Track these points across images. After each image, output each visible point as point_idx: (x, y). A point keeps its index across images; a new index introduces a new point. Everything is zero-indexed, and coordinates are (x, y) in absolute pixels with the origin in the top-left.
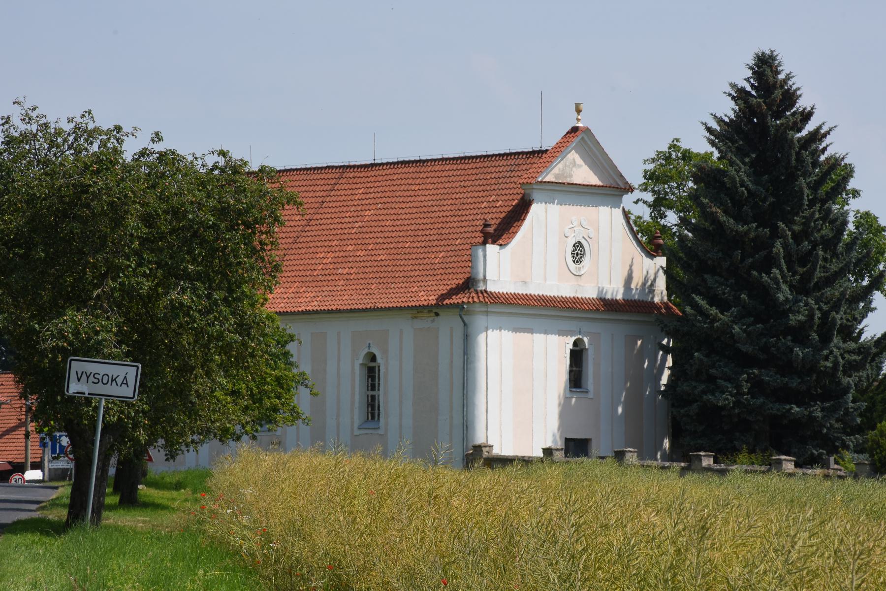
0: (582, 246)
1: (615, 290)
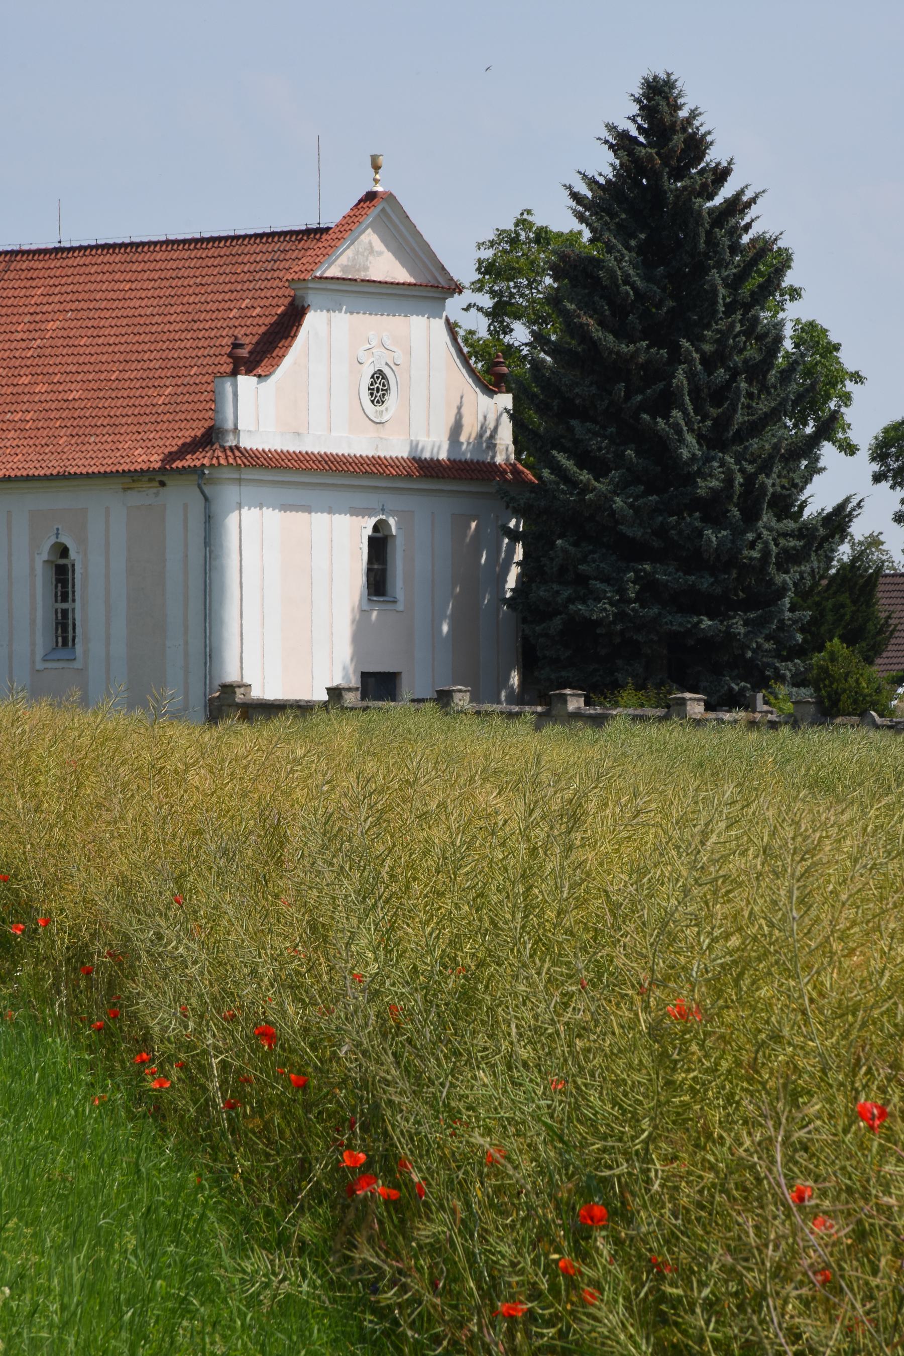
0: (384, 377)
1: (436, 446)
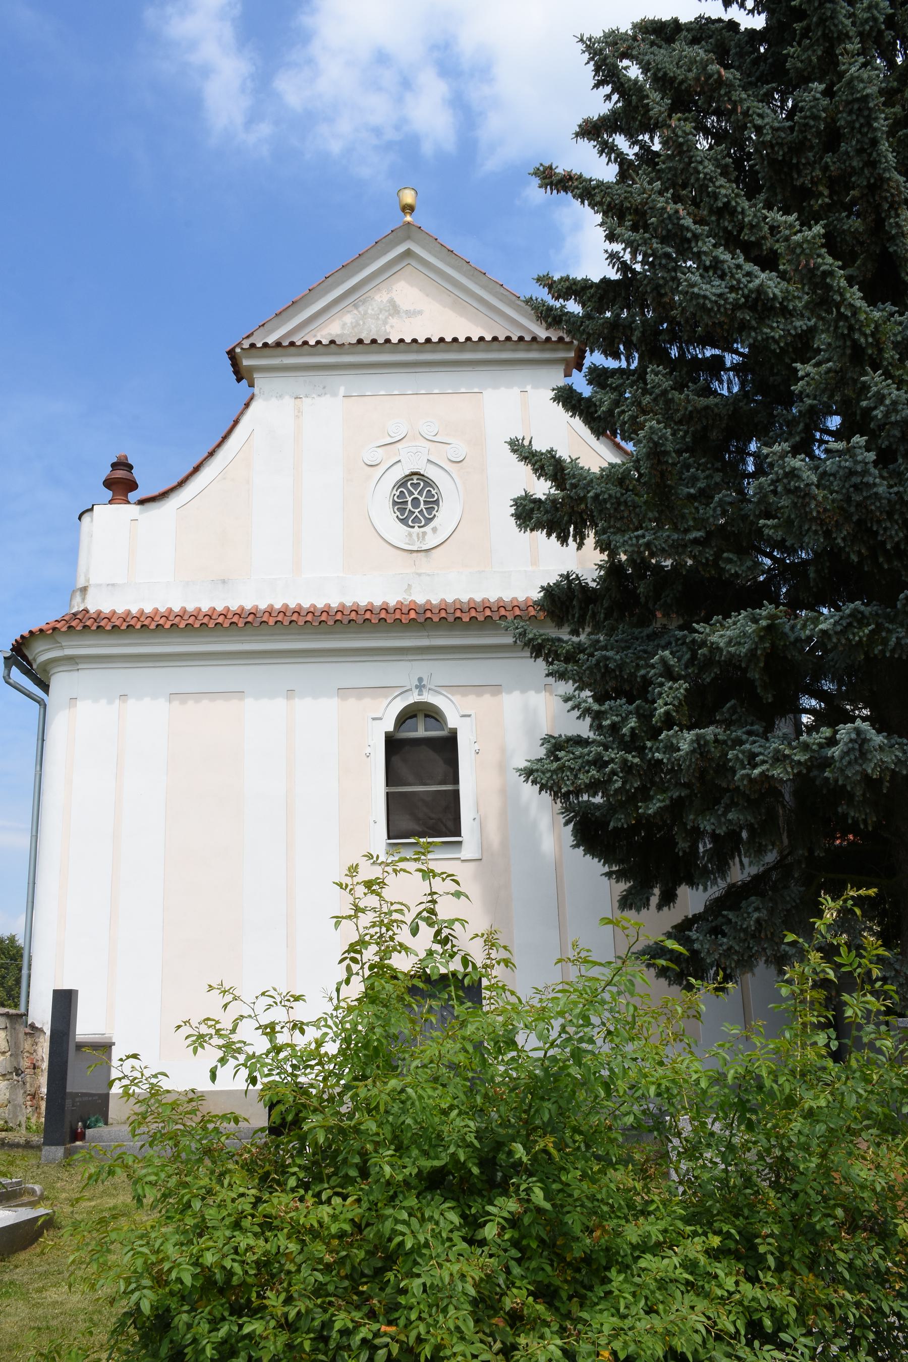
0: (429, 483)
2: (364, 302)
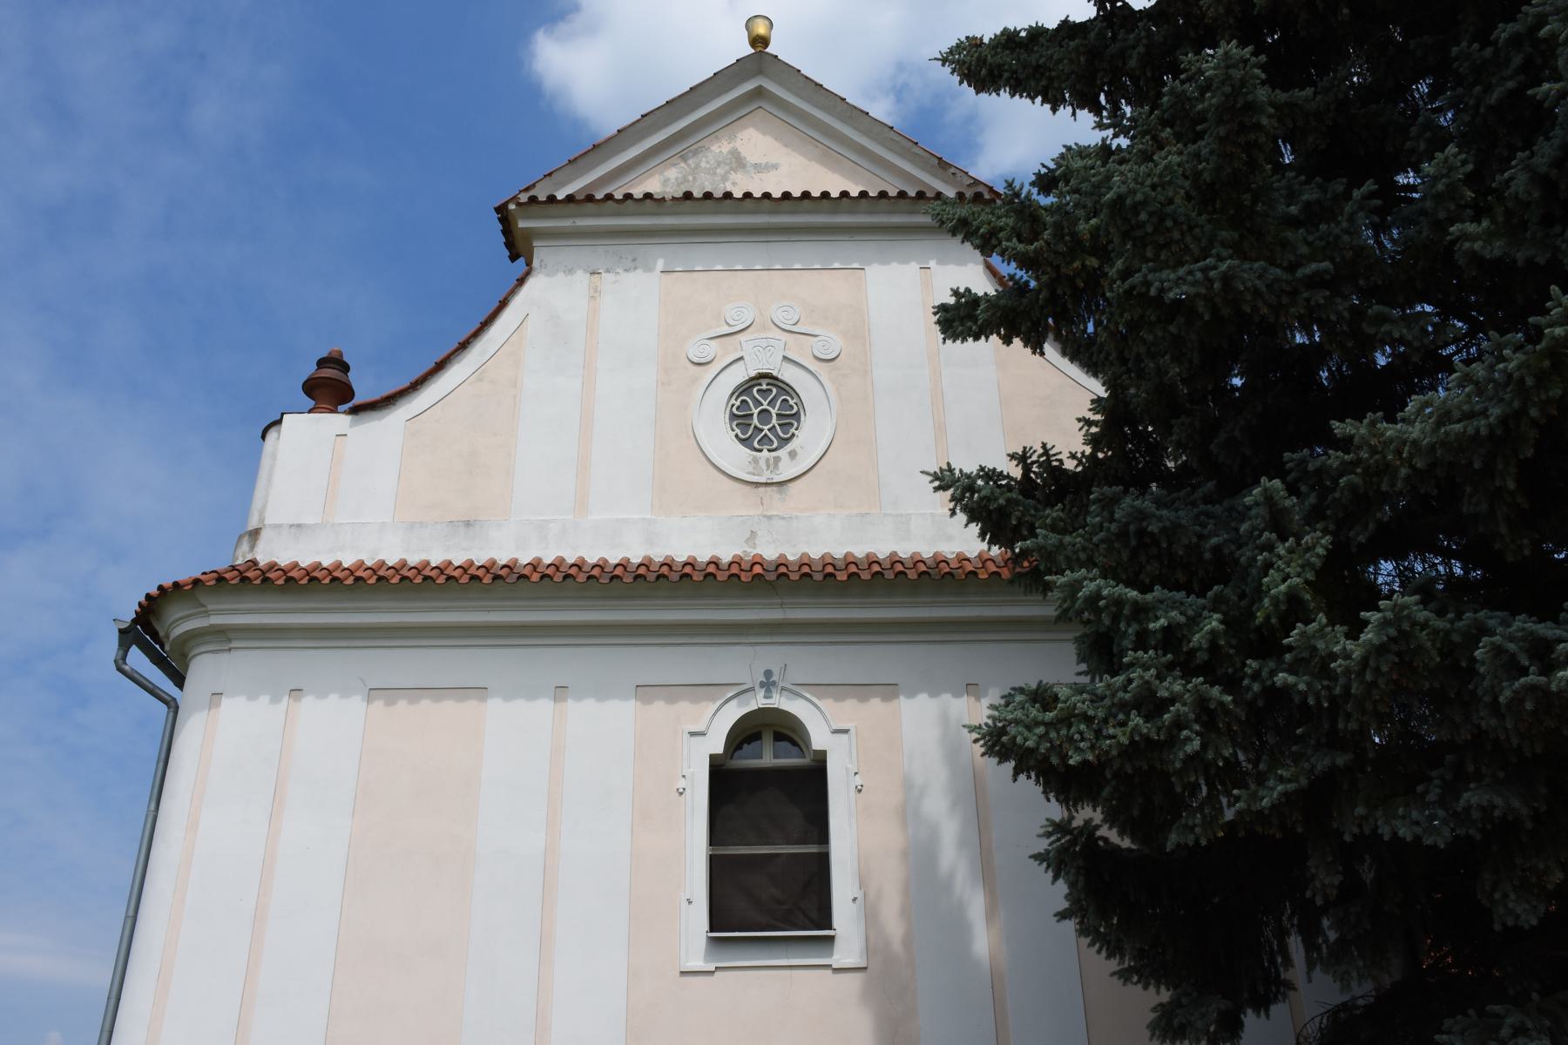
0: (785, 388)
2: (695, 153)
